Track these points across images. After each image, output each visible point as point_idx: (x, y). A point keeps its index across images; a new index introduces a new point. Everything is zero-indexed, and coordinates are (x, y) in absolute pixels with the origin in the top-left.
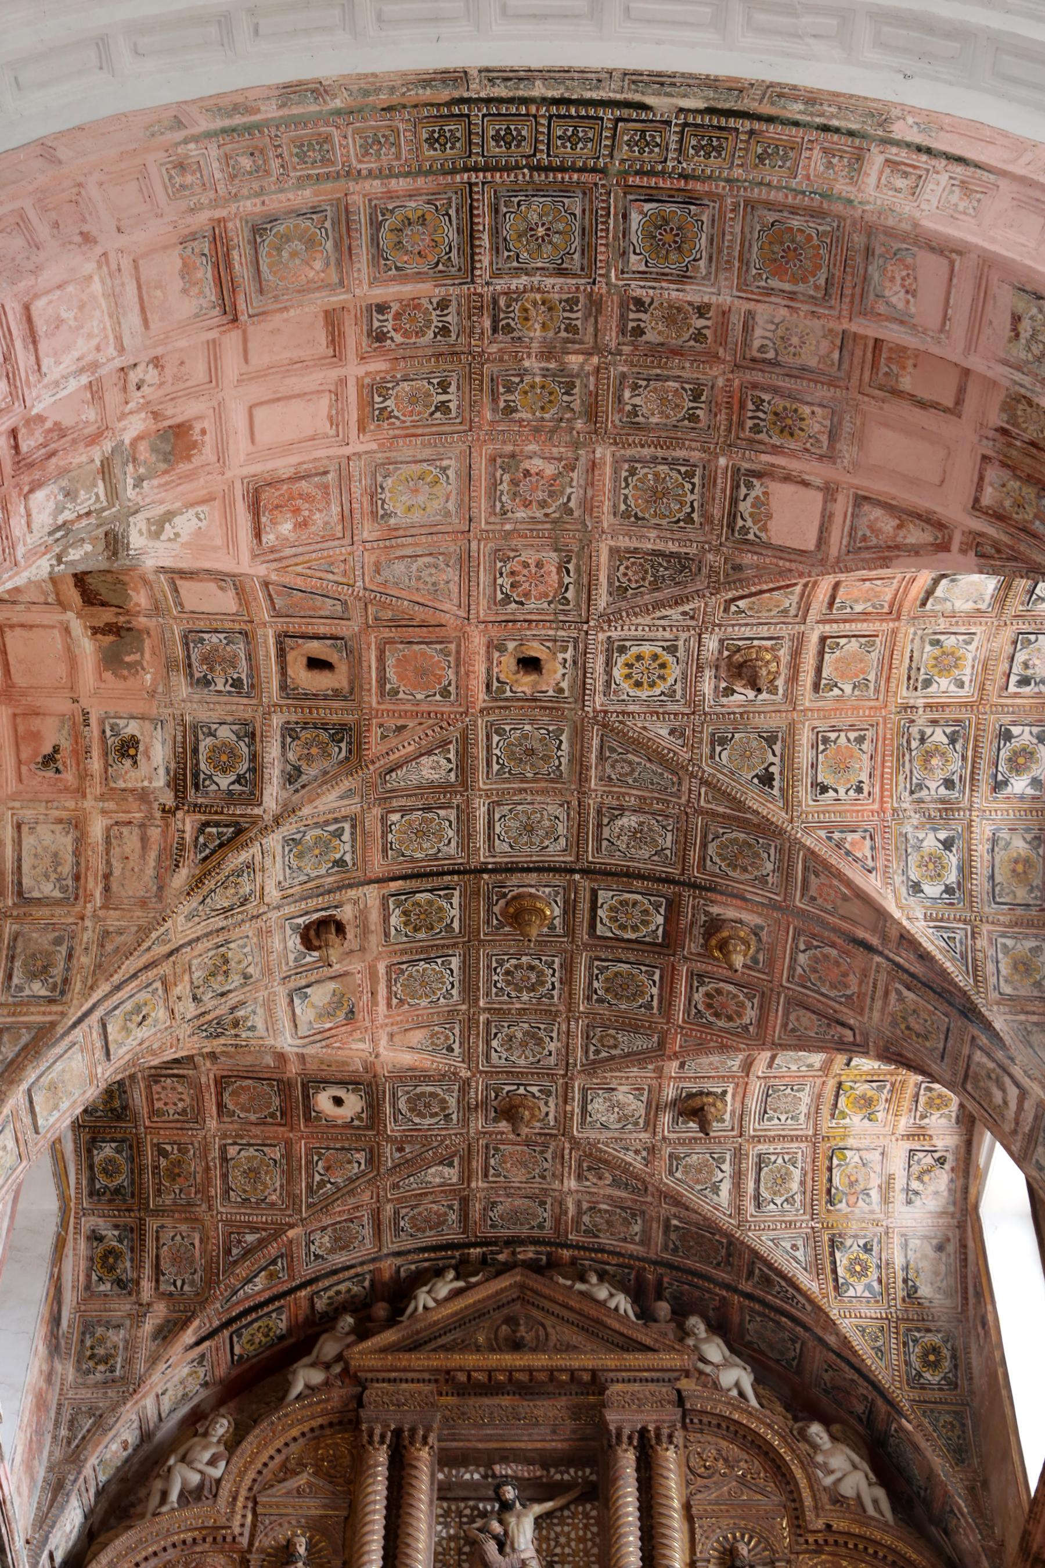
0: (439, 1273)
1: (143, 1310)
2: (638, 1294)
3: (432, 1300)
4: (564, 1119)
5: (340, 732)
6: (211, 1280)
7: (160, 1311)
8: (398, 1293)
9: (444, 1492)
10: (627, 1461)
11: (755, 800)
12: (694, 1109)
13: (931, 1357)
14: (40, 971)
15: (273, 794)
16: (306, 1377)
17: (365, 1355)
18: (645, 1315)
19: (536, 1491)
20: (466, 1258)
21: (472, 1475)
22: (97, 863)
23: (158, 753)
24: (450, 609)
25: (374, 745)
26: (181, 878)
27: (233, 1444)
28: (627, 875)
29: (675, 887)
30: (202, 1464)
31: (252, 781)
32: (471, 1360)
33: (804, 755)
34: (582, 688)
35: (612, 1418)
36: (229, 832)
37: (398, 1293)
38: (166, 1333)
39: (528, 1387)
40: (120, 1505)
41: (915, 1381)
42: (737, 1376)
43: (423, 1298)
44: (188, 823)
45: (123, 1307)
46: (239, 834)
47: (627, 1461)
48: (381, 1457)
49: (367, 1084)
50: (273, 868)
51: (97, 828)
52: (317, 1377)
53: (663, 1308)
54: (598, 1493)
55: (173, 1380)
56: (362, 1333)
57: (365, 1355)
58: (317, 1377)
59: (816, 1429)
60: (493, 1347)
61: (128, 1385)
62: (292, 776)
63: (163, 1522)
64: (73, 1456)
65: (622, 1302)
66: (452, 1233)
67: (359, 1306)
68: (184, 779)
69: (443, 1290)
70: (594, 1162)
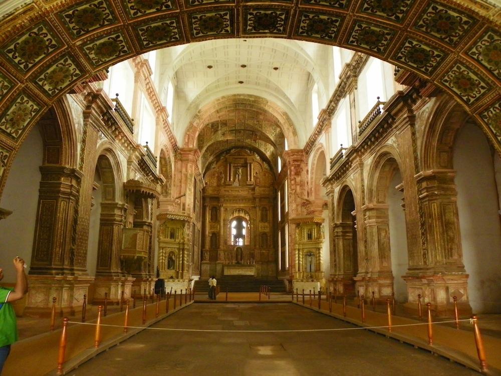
0: (232, 149)
1: (208, 154)
2: (250, 150)
3: (233, 151)
4: (243, 141)
5: (225, 124)
6: (214, 152)
7: (210, 154)
8: (230, 150)
9: (234, 166)
10: (249, 165)
11: (259, 129)
12: (255, 141)
13: (274, 158)
14: (201, 141)
15: (220, 128)
16: (222, 158)
17: (226, 156)
18: (251, 153)
19: (242, 166)
20: (236, 147)
21: (236, 165)
22: (205, 132)
23: (210, 125)
24: (234, 119)
25: (228, 125)
26: (213, 133)
27: (216, 163)
28: (248, 130)
29: (253, 131)
30: (214, 166)
31: (218, 127)
32: (236, 157)
33: (263, 126)
34: (245, 122)
35: (248, 161)
36: (216, 131)
37: (230, 150)
38: (210, 155)
39: (240, 158)
40: (208, 169)
41: (272, 160)
42: (258, 158)
43: (232, 151)
44: (213, 130)
45: (206, 153)
46: (217, 131)
47: (249, 165)
48: (228, 165)
49: (227, 140)
50: (220, 132)
51: (205, 130)
52: (223, 158)
53: (252, 152)
54: (246, 167)
55: (211, 159)
56: (227, 154)
57: (226, 156)
58: (223, 158)
59: (264, 163)
60: (238, 155)
61: (208, 160)
62: (221, 127)
63: (211, 170)
64: (204, 166)
65: (249, 151)
66: (234, 145)
67: (226, 151)
68: (212, 126)
69: (233, 150)
70: (245, 143)
